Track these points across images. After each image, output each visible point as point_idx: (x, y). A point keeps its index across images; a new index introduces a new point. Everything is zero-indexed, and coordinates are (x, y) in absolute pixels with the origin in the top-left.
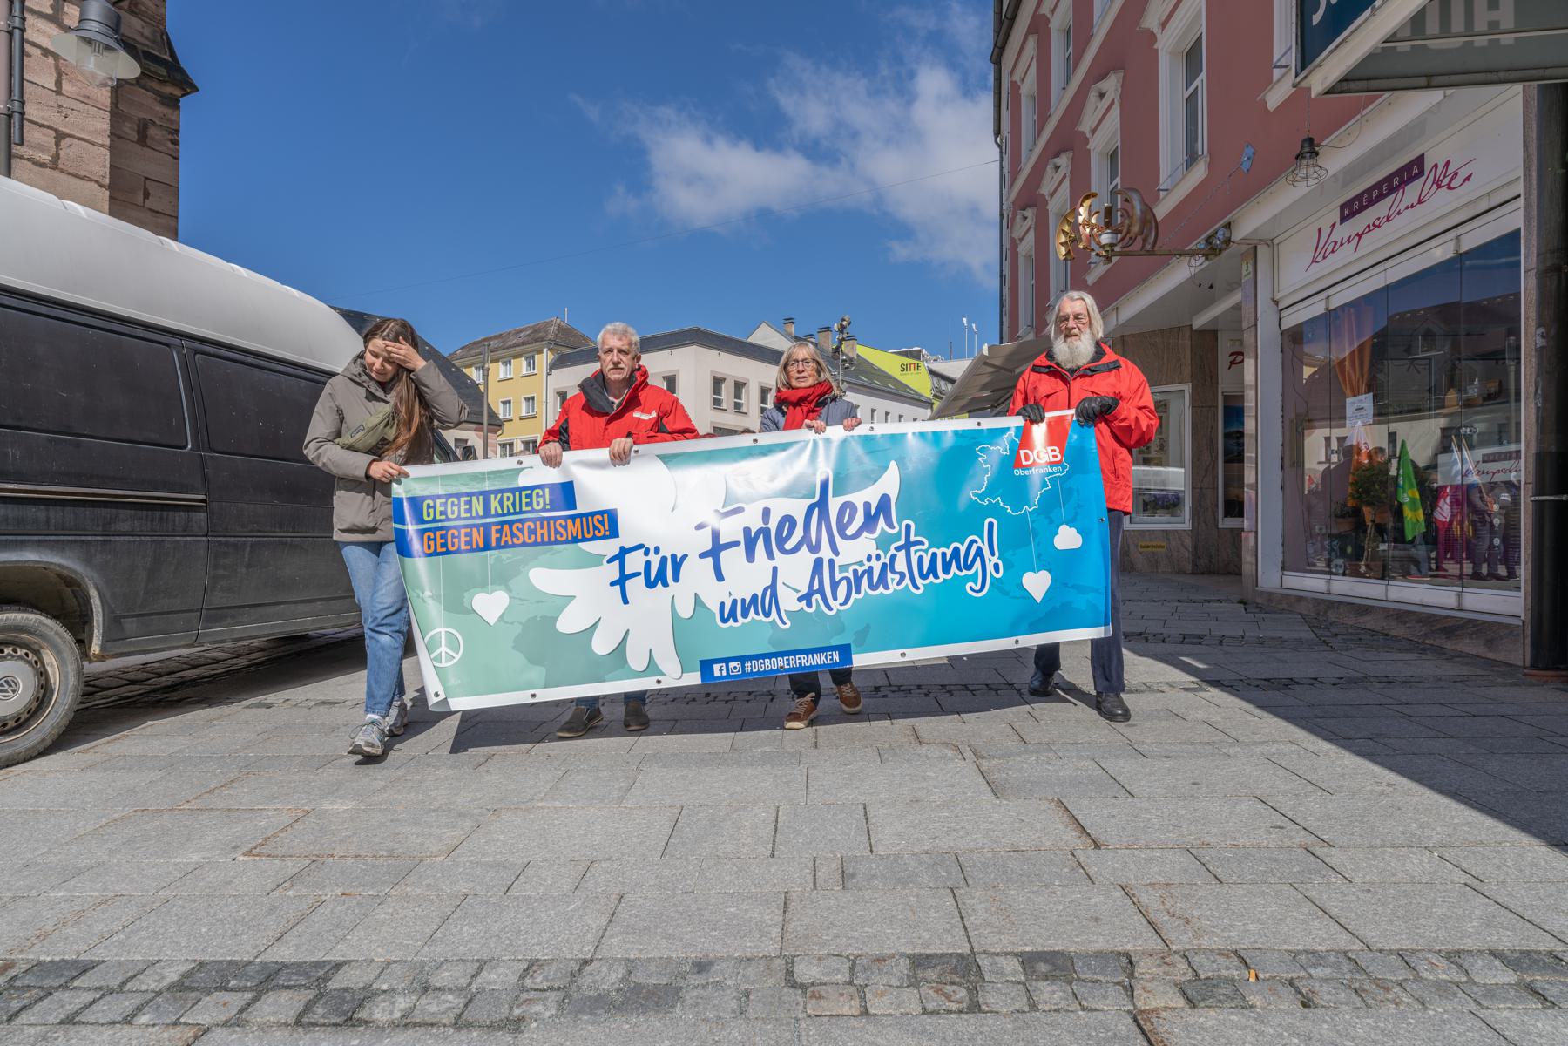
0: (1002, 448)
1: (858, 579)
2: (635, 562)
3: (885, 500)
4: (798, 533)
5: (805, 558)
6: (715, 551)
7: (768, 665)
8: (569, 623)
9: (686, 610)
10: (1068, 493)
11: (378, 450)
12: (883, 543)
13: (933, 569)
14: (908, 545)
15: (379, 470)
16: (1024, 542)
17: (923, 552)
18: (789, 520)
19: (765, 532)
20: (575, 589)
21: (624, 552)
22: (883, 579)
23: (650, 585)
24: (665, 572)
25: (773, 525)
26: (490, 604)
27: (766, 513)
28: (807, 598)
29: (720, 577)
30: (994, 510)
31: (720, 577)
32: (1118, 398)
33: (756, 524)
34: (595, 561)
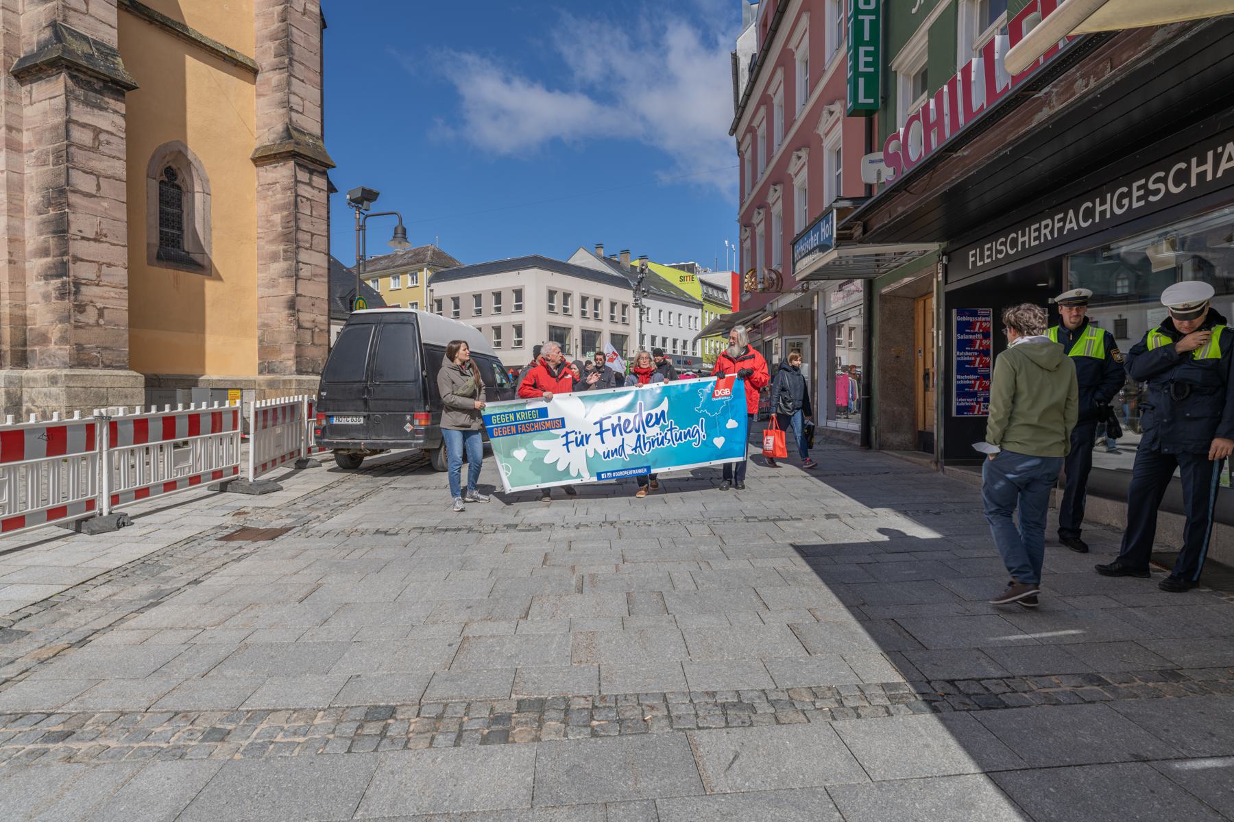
0: (708, 389)
2: (572, 437)
3: (663, 412)
4: (632, 425)
5: (635, 434)
6: (601, 433)
7: (621, 474)
8: (548, 460)
9: (591, 455)
10: (732, 407)
11: (473, 396)
12: (662, 428)
14: (671, 429)
15: (477, 404)
16: (714, 426)
17: (677, 432)
18: (628, 421)
20: (550, 447)
21: (567, 433)
22: (662, 442)
24: (583, 441)
26: (520, 454)
28: (635, 449)
30: (703, 415)
32: (754, 369)
33: (616, 422)
34: (556, 437)
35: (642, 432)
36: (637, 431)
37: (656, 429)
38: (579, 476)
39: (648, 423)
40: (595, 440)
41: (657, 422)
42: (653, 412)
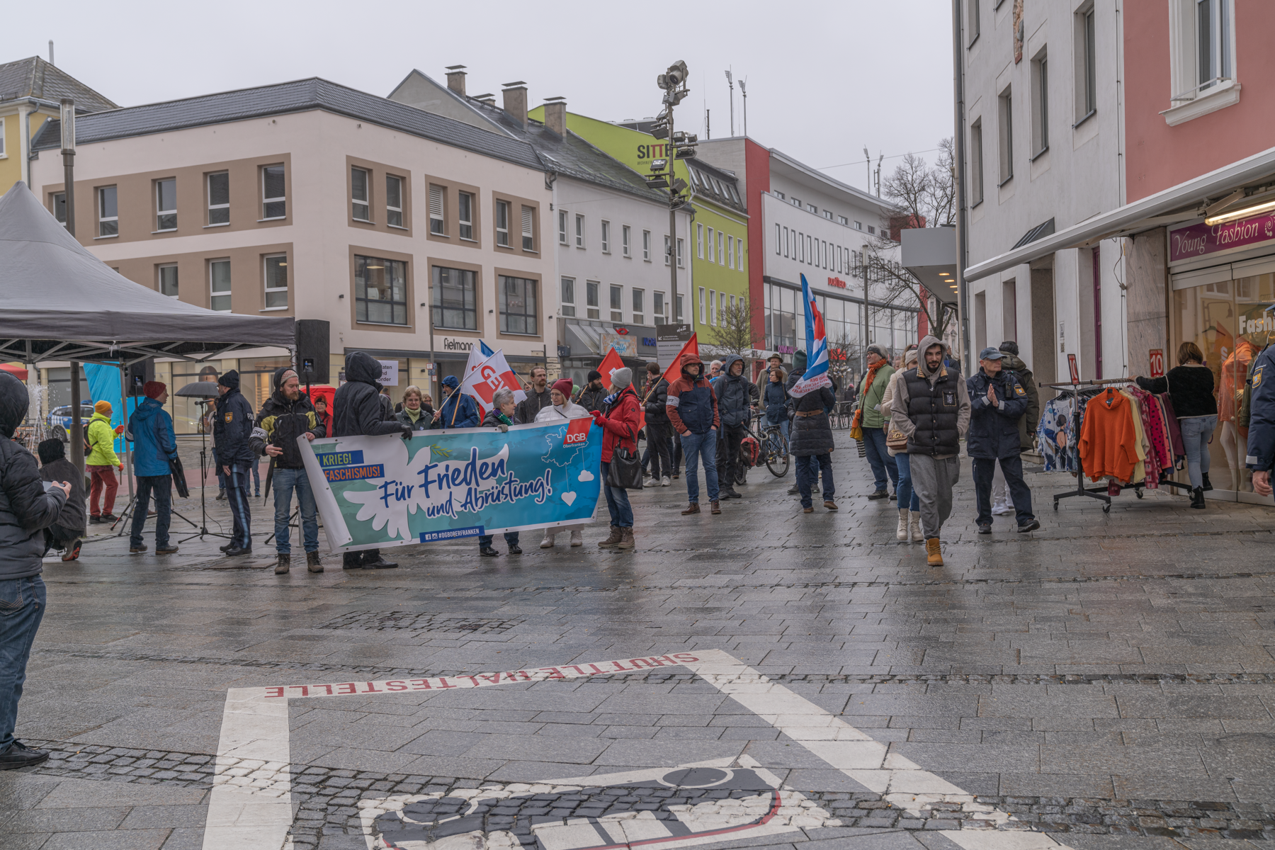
1: (487, 497)
3: (502, 461)
5: (464, 487)
6: (425, 485)
8: (362, 516)
9: (413, 511)
12: (499, 481)
13: (520, 493)
18: (457, 470)
19: (447, 476)
20: (367, 500)
21: (387, 484)
23: (398, 499)
25: (450, 473)
27: (447, 467)
28: (464, 505)
29: (428, 496)
31: (428, 496)
33: (443, 472)
34: (373, 487)
35: (473, 485)
36: (468, 484)
37: (492, 482)
38: (399, 537)
39: (482, 474)
40: (418, 493)
41: (494, 473)
42: (489, 461)
